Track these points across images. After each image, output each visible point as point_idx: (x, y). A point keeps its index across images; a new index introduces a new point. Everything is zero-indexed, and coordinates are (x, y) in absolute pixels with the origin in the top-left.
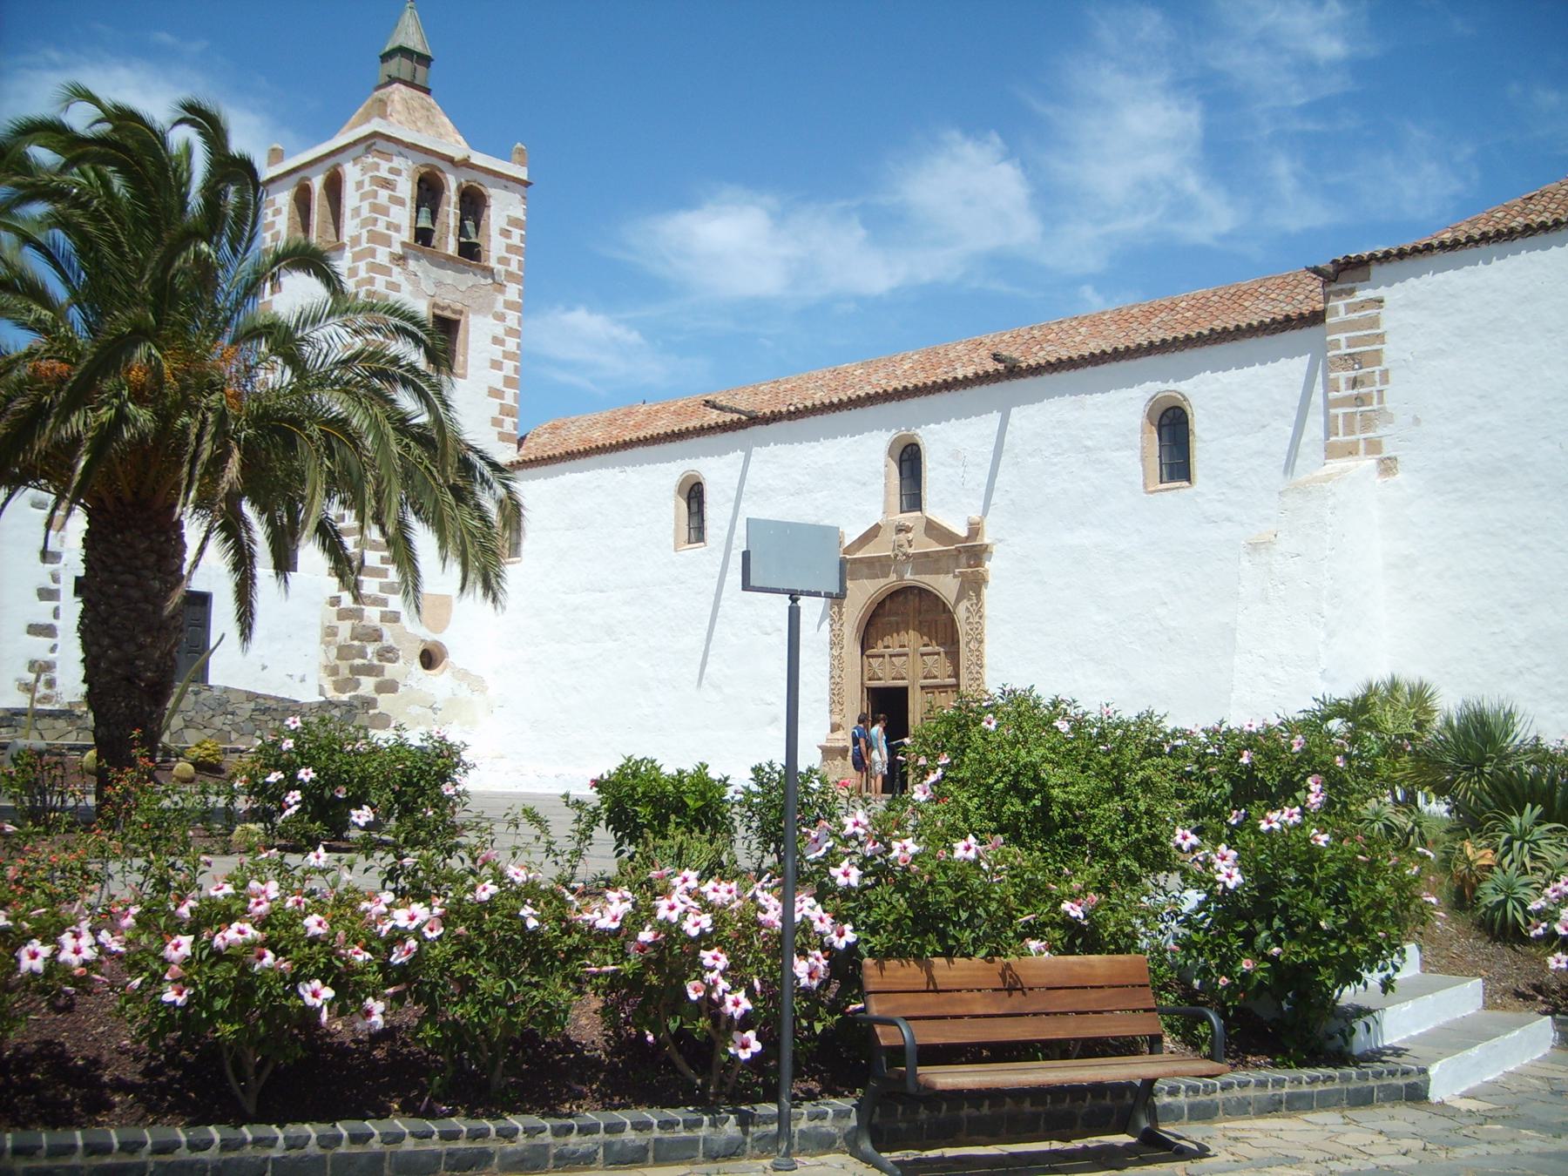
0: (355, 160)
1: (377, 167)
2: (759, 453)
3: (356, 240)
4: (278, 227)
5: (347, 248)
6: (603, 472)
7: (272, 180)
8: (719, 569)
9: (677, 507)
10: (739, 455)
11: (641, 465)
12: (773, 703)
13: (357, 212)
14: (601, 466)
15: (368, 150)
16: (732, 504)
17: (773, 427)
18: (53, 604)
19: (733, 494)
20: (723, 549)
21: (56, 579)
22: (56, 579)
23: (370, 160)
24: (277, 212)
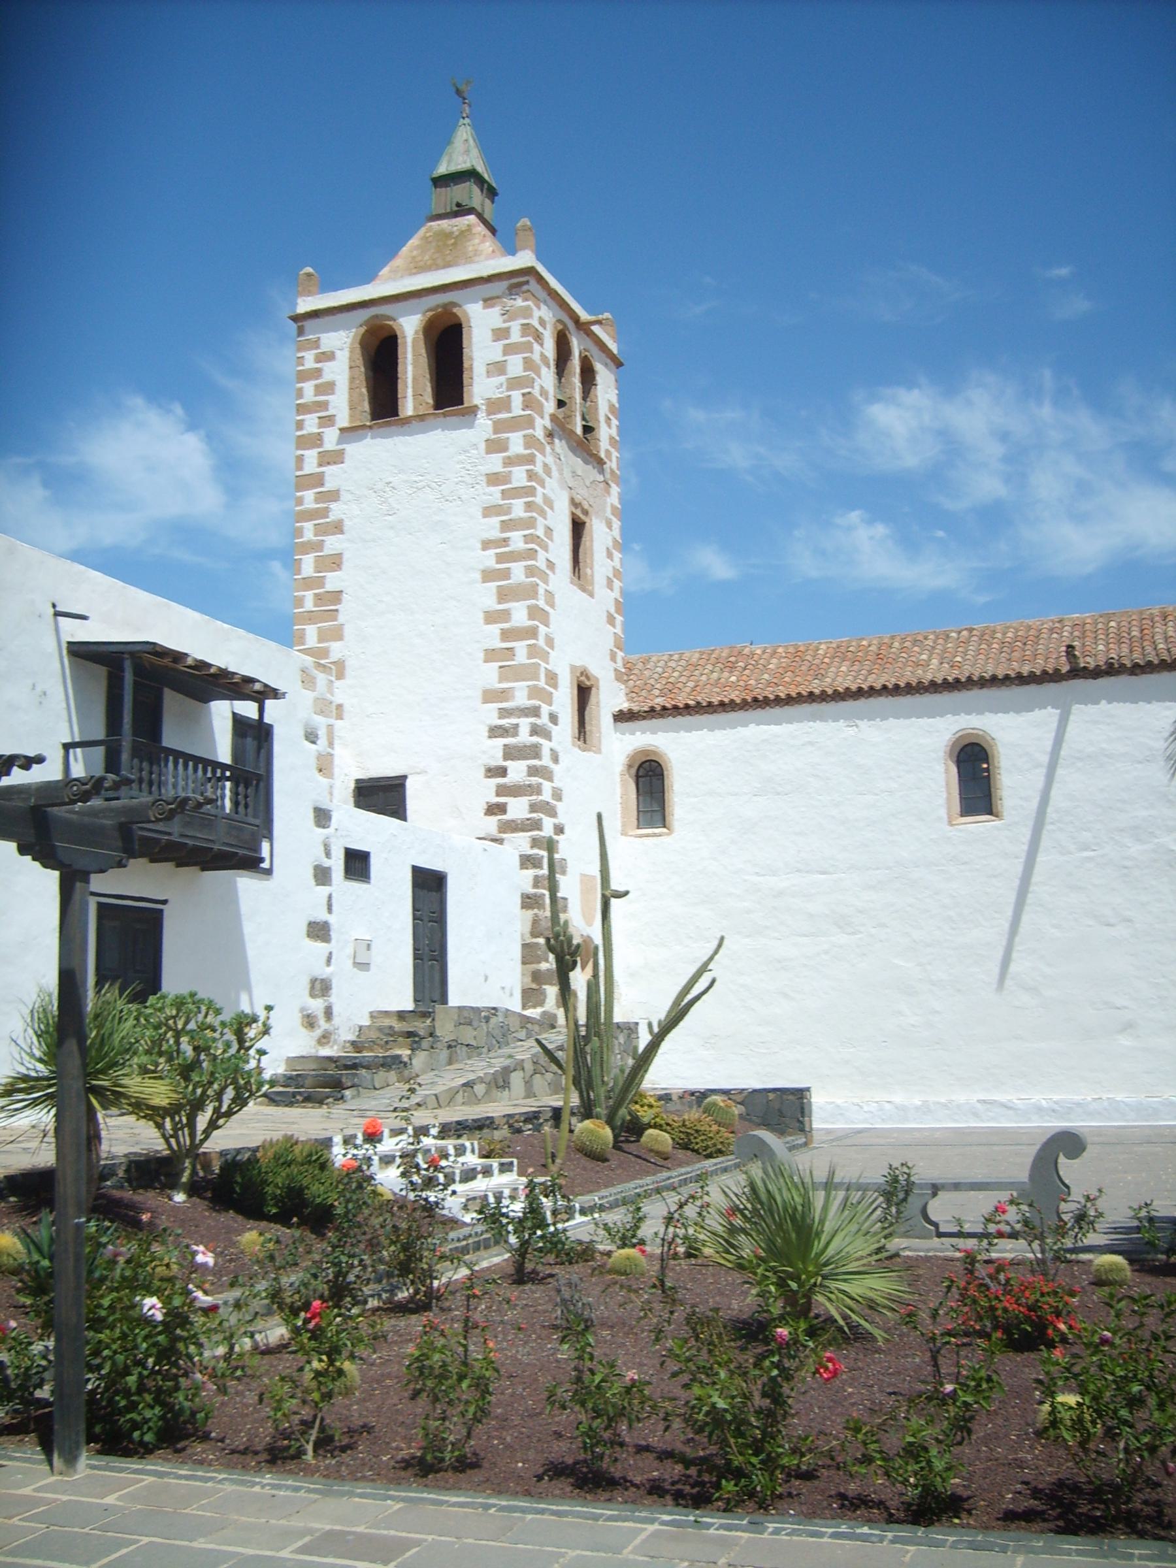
0: (488, 301)
1: (526, 312)
2: (1081, 714)
3: (497, 405)
4: (327, 377)
5: (481, 415)
6: (818, 725)
7: (315, 314)
8: (1025, 847)
9: (947, 771)
10: (1050, 715)
11: (884, 718)
12: (1125, 1007)
13: (497, 368)
14: (814, 718)
15: (514, 290)
16: (1043, 771)
17: (1103, 682)
18: (324, 890)
19: (1045, 759)
20: (1031, 823)
21: (328, 854)
22: (328, 854)
23: (519, 302)
24: (329, 356)
